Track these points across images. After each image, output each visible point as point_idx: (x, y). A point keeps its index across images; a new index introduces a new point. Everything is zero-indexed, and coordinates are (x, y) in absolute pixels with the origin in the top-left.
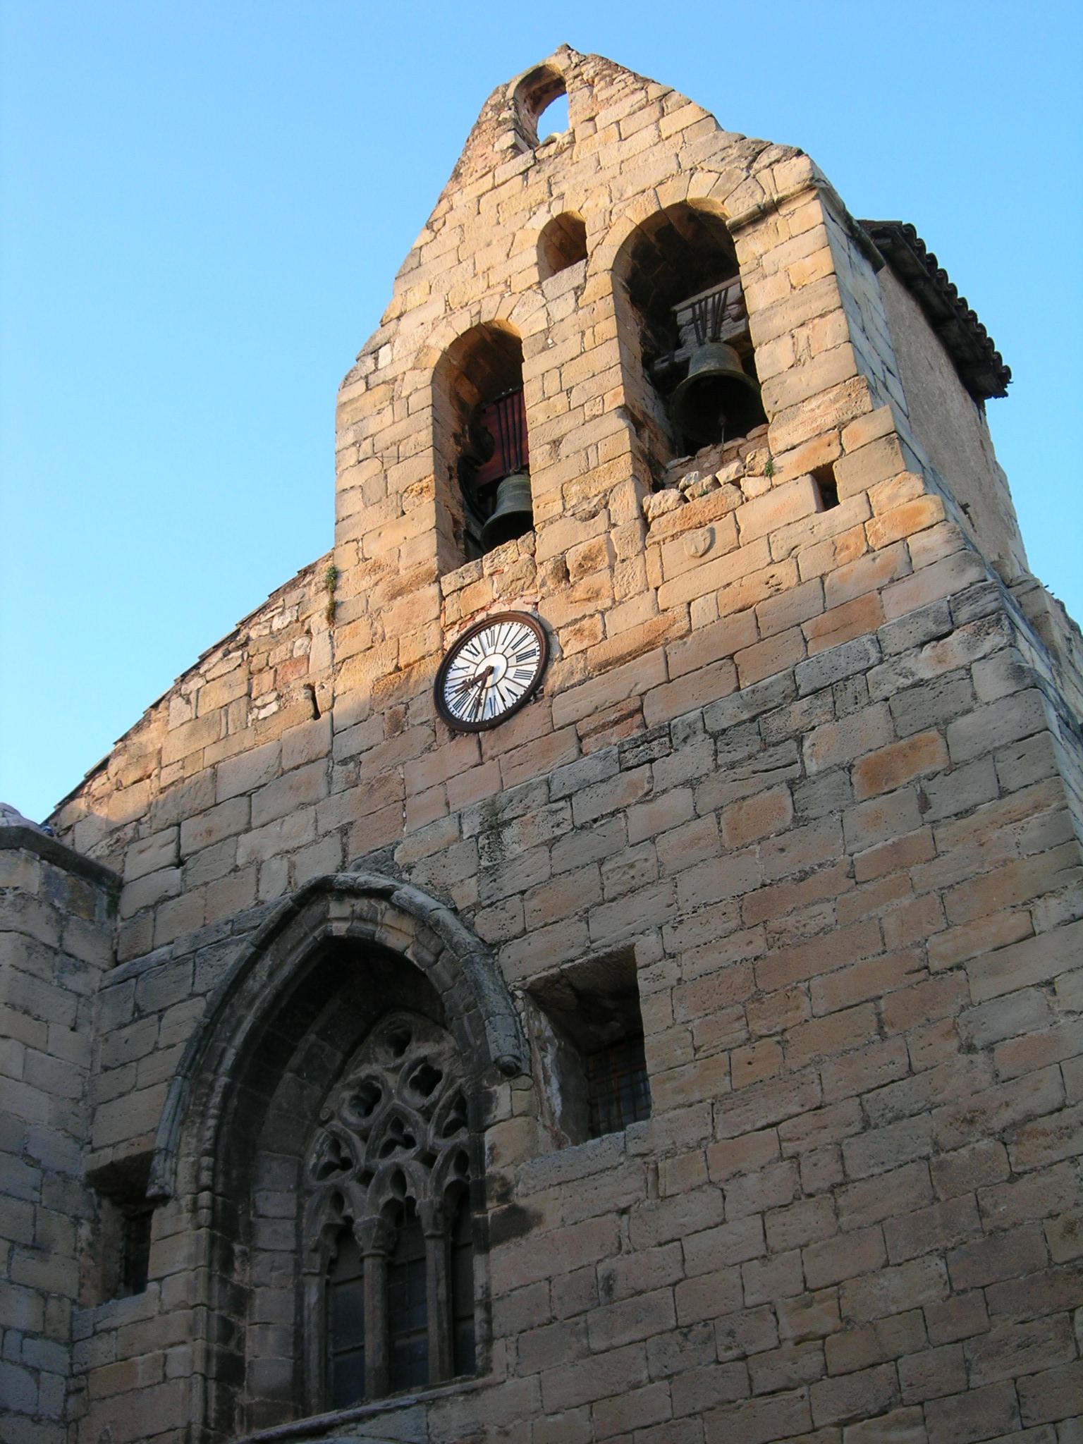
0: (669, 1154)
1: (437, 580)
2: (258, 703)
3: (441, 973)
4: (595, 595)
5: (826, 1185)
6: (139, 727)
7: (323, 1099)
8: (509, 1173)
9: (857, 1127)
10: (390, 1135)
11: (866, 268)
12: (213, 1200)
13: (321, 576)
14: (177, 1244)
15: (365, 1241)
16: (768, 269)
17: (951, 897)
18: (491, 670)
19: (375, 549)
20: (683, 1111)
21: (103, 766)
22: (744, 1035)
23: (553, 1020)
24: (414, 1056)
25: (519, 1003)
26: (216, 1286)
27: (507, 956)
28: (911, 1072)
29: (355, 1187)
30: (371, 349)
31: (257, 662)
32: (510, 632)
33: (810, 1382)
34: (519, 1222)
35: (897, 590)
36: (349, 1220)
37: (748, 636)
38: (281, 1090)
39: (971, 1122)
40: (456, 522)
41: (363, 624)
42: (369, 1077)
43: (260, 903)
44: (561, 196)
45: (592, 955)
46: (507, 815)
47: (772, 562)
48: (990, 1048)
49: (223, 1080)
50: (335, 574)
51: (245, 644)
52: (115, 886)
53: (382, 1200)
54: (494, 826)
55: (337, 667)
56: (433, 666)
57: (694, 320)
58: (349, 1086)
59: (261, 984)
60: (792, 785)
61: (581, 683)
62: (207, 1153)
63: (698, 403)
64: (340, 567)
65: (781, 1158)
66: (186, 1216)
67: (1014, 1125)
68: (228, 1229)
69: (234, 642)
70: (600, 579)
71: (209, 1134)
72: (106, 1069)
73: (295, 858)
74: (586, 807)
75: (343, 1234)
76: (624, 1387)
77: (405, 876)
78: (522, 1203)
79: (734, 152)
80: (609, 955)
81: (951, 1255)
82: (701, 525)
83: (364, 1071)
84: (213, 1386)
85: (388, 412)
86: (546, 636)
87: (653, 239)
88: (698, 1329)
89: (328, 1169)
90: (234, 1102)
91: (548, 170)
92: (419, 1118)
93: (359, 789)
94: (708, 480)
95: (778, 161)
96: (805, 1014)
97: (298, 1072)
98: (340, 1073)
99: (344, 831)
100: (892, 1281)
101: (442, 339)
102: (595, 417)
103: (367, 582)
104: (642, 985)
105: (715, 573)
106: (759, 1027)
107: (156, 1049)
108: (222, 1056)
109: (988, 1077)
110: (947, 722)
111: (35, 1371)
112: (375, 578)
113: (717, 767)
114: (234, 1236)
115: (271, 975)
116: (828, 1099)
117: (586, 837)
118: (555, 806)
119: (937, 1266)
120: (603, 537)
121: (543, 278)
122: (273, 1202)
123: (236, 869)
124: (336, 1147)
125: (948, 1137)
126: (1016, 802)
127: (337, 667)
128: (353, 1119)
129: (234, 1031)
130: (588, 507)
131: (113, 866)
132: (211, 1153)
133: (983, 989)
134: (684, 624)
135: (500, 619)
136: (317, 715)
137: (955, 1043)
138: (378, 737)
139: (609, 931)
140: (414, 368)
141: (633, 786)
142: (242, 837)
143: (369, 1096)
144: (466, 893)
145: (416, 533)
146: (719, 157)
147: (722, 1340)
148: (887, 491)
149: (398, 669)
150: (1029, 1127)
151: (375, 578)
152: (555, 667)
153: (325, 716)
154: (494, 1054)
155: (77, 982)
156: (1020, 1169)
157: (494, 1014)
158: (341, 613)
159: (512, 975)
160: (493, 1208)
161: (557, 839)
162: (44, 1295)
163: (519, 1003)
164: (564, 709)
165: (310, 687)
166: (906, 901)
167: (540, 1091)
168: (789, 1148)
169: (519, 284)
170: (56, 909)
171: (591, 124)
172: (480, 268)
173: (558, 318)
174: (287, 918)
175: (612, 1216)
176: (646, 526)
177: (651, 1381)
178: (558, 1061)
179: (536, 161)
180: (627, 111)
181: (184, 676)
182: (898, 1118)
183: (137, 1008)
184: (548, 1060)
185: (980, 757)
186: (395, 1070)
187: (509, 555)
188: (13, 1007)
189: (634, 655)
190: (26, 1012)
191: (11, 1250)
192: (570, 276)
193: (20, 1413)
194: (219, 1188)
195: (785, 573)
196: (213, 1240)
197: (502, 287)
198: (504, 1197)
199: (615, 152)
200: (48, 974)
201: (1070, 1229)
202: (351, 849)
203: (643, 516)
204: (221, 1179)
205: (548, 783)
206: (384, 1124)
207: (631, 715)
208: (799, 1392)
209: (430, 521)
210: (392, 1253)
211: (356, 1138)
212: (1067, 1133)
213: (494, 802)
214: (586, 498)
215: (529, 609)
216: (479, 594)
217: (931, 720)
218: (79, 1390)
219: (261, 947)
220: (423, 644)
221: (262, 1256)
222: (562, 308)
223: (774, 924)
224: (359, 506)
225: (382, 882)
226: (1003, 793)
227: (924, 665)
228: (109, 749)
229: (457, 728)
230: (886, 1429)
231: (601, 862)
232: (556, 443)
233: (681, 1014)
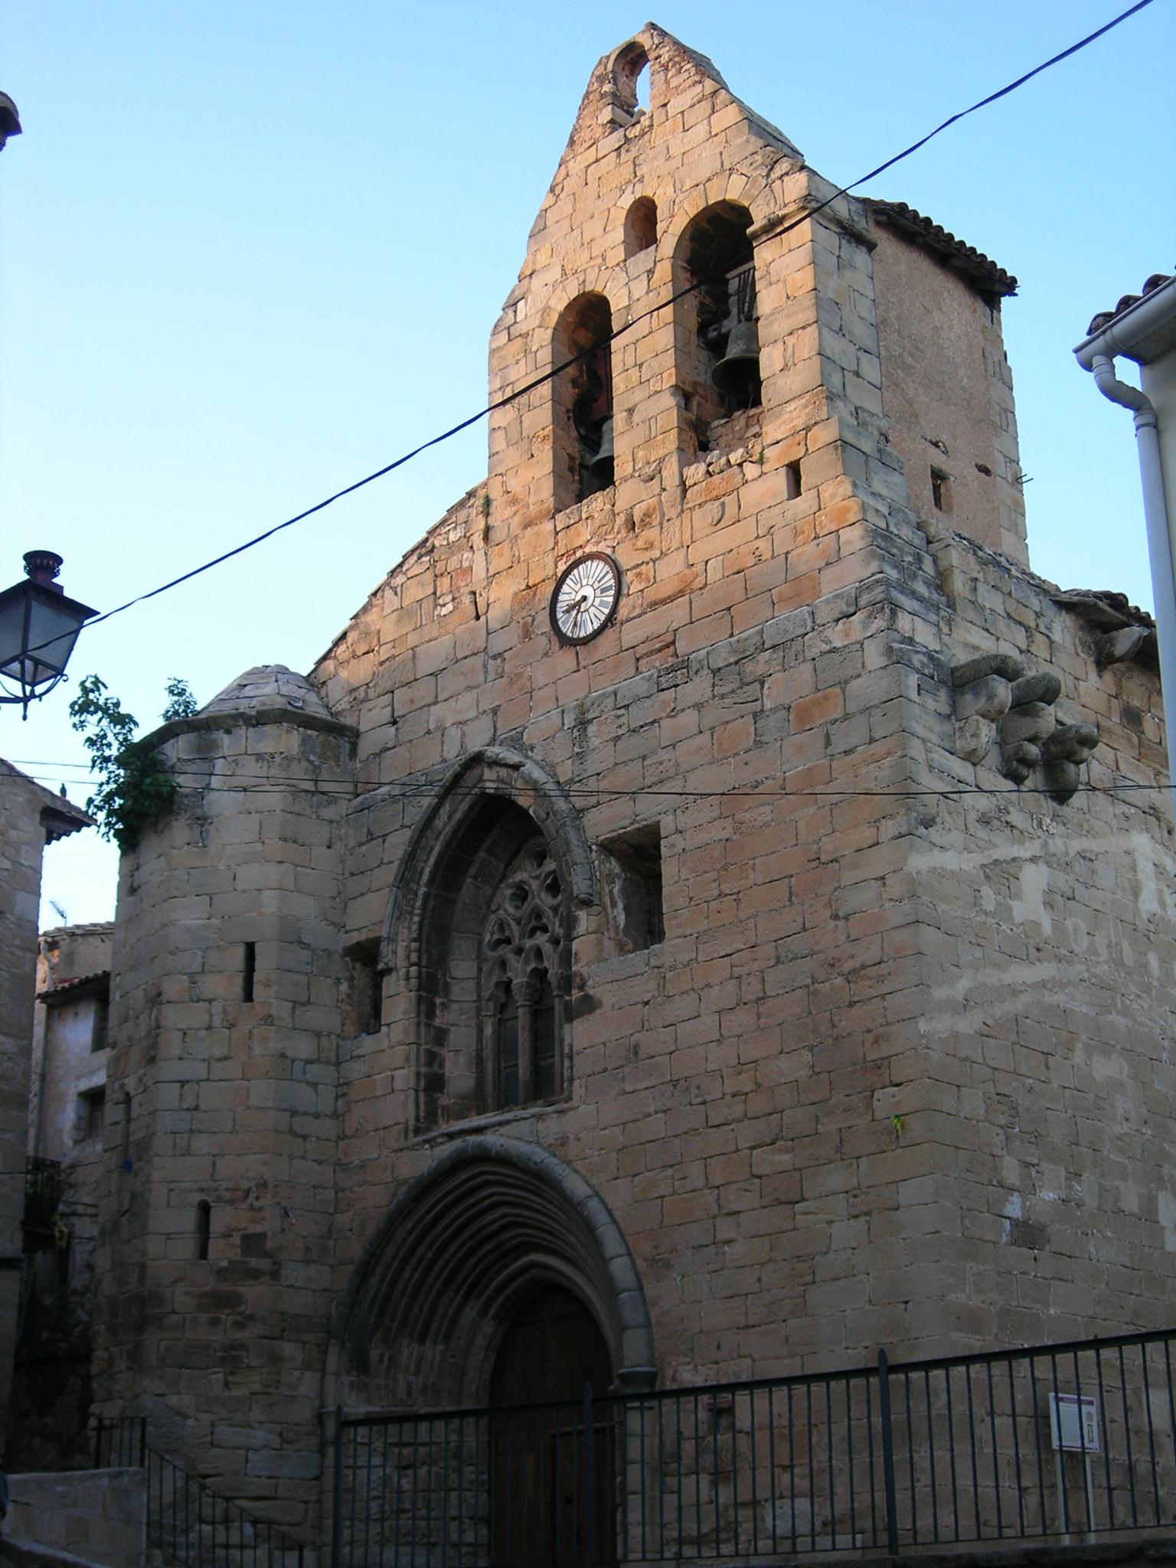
0: (672, 968)
1: (553, 517)
2: (441, 601)
3: (550, 826)
4: (650, 546)
5: (754, 998)
6: (365, 609)
7: (493, 895)
8: (584, 971)
9: (773, 962)
10: (534, 923)
11: (860, 257)
12: (420, 972)
13: (479, 502)
14: (399, 1001)
15: (519, 996)
16: (774, 279)
17: (836, 812)
18: (584, 598)
19: (515, 485)
20: (679, 940)
21: (344, 636)
22: (717, 892)
23: (619, 860)
24: (547, 869)
25: (594, 854)
26: (423, 1030)
27: (589, 819)
28: (804, 929)
29: (511, 957)
30: (512, 302)
31: (440, 567)
32: (597, 568)
34: (589, 1005)
35: (828, 573)
36: (510, 981)
37: (739, 595)
38: (464, 891)
39: (833, 965)
40: (572, 458)
41: (506, 545)
42: (521, 881)
43: (444, 760)
44: (641, 180)
45: (636, 826)
46: (590, 716)
47: (758, 537)
48: (846, 918)
49: (423, 890)
50: (488, 502)
51: (432, 551)
52: (353, 735)
53: (529, 969)
54: (583, 724)
55: (491, 578)
56: (548, 589)
57: (738, 292)
58: (509, 887)
59: (444, 824)
60: (755, 716)
61: (639, 616)
62: (414, 940)
63: (724, 386)
64: (492, 497)
65: (731, 978)
66: (402, 982)
67: (855, 970)
68: (430, 989)
69: (423, 548)
70: (652, 533)
71: (415, 927)
72: (352, 874)
73: (465, 728)
74: (638, 715)
75: (507, 986)
77: (530, 753)
78: (591, 992)
79: (758, 158)
80: (646, 826)
81: (815, 1050)
82: (717, 498)
83: (519, 876)
84: (422, 1095)
85: (522, 362)
86: (619, 575)
87: (706, 225)
88: (682, 1082)
89: (499, 942)
90: (431, 903)
91: (634, 153)
92: (550, 913)
93: (504, 680)
94: (723, 460)
95: (787, 174)
96: (750, 882)
97: (475, 878)
98: (503, 877)
99: (495, 711)
100: (783, 1063)
101: (559, 304)
102: (657, 392)
103: (509, 512)
104: (663, 851)
105: (724, 539)
106: (726, 888)
107: (382, 863)
108: (421, 873)
109: (843, 938)
110: (846, 682)
111: (315, 1085)
112: (514, 509)
113: (714, 696)
114: (436, 993)
115: (450, 817)
116: (759, 941)
117: (636, 739)
118: (619, 712)
119: (807, 1056)
120: (656, 499)
121: (630, 253)
122: (462, 968)
123: (429, 732)
124: (502, 928)
125: (820, 974)
126: (878, 748)
127: (491, 578)
128: (511, 910)
129: (429, 855)
130: (649, 471)
131: (348, 721)
132: (418, 940)
133: (848, 878)
134: (701, 579)
135: (591, 557)
136: (478, 618)
137: (828, 912)
138: (515, 641)
139: (647, 809)
140: (540, 326)
141: (665, 703)
142: (432, 708)
143: (521, 894)
144: (566, 771)
145: (537, 476)
146: (748, 162)
147: (694, 1091)
148: (830, 490)
149: (528, 587)
150: (863, 972)
151: (514, 509)
152: (623, 601)
153: (483, 618)
154: (576, 892)
155: (329, 813)
156: (856, 999)
157: (576, 864)
158: (492, 535)
159: (590, 834)
160: (576, 994)
161: (618, 737)
162: (318, 1035)
163: (594, 854)
164: (631, 634)
165: (474, 593)
166: (811, 811)
167: (607, 914)
168: (737, 971)
169: (611, 263)
170: (311, 762)
171: (663, 111)
172: (586, 239)
173: (635, 297)
174: (457, 778)
175: (640, 1006)
176: (685, 491)
178: (624, 890)
179: (627, 140)
180: (690, 102)
181: (393, 572)
182: (795, 958)
183: (370, 832)
184: (615, 890)
185: (862, 712)
186: (537, 877)
187: (597, 503)
188: (285, 840)
189: (671, 599)
190: (295, 842)
191: (294, 1008)
192: (644, 259)
193: (306, 1113)
194: (424, 963)
195: (764, 545)
196: (419, 999)
197: (599, 260)
198: (581, 988)
199: (679, 142)
200: (308, 811)
201: (876, 1040)
202: (499, 726)
203: (683, 483)
204: (425, 956)
205: (615, 693)
206: (530, 916)
207: (667, 646)
208: (733, 1126)
209: (548, 467)
210: (538, 1003)
211: (513, 923)
212: (881, 979)
213: (582, 704)
214: (648, 463)
215: (609, 551)
216: (578, 534)
217: (837, 680)
218: (344, 1095)
219: (442, 798)
220: (545, 568)
221: (454, 1006)
222: (639, 288)
223: (739, 817)
224: (504, 445)
225: (514, 758)
226: (872, 740)
227: (837, 636)
228: (346, 623)
229: (565, 641)
231: (644, 758)
232: (631, 411)
233: (684, 874)
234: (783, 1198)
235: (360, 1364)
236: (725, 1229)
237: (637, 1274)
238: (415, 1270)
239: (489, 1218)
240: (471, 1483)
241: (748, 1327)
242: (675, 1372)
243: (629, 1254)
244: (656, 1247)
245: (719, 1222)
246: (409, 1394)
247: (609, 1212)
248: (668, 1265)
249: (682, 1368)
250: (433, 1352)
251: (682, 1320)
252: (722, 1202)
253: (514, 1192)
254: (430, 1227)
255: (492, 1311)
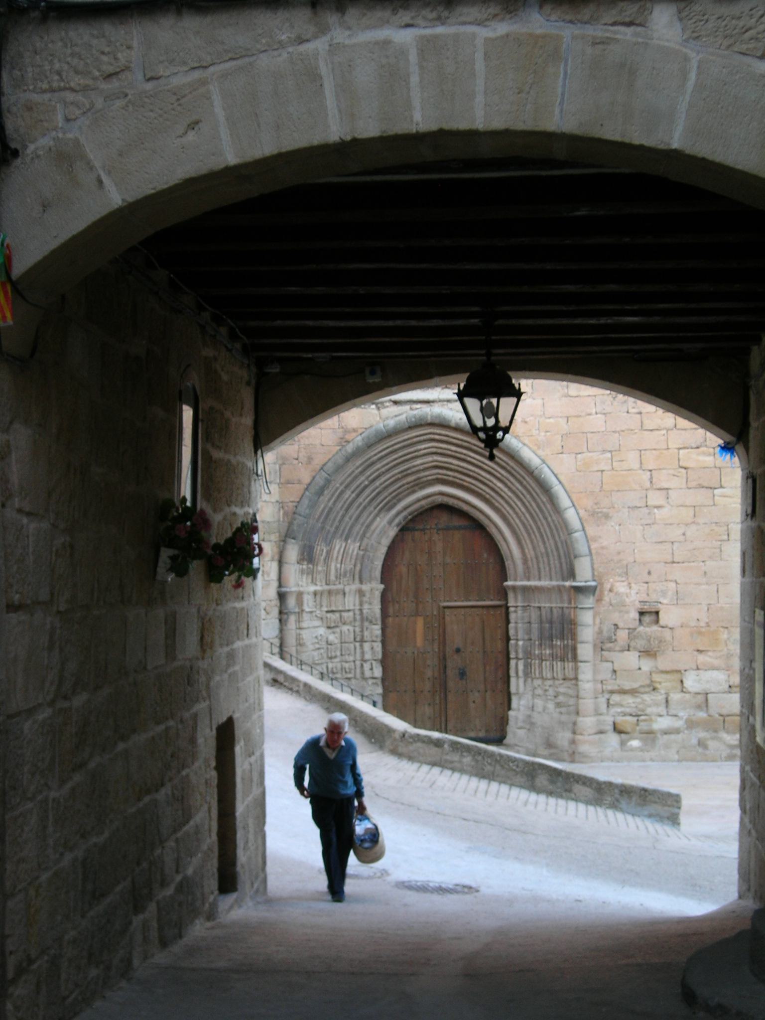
33: (668, 430)
76: (583, 414)
177: (596, 413)
230: (698, 454)
234: (706, 484)
235: (308, 556)
236: (655, 498)
237: (580, 519)
238: (353, 492)
239: (419, 461)
240: (377, 637)
241: (673, 562)
242: (612, 586)
243: (574, 506)
244: (596, 504)
245: (650, 494)
246: (336, 577)
247: (556, 476)
248: (607, 517)
249: (618, 584)
250: (354, 547)
251: (619, 553)
252: (654, 480)
253: (454, 448)
254: (373, 464)
255: (397, 521)
